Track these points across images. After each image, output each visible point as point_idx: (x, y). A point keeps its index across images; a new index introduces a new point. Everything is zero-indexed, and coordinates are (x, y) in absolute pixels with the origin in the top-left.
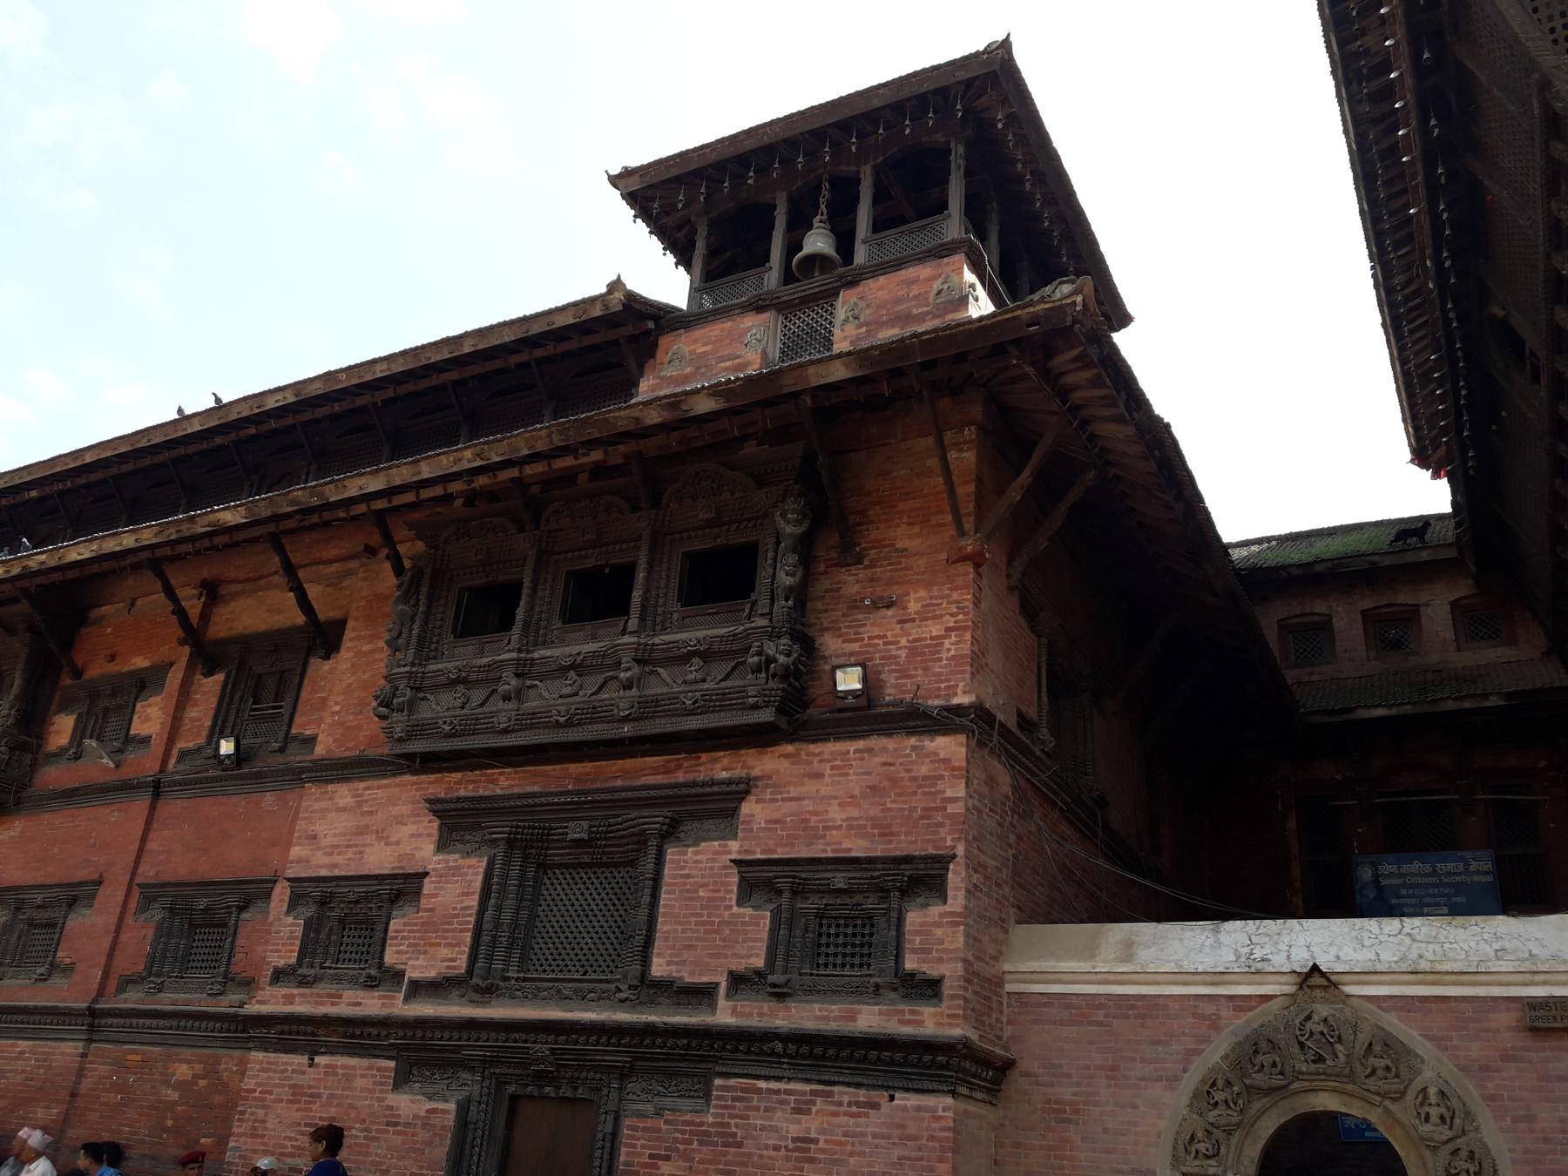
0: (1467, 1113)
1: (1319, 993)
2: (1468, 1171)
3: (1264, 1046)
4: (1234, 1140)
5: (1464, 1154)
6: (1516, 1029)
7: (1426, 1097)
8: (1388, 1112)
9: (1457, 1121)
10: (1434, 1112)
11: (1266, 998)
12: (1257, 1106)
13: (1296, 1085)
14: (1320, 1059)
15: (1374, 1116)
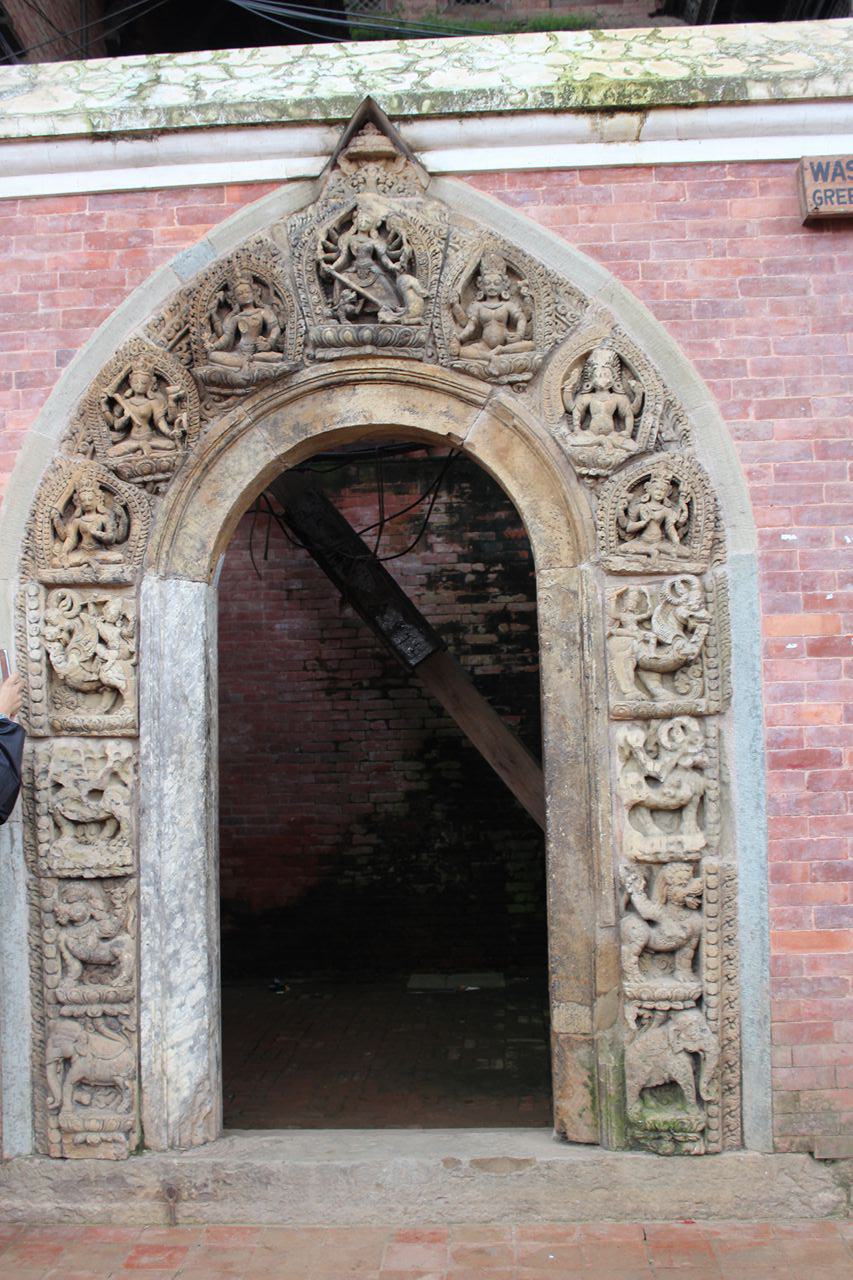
0: (669, 405)
1: (372, 171)
2: (663, 524)
3: (244, 289)
4: (163, 503)
5: (658, 488)
6: (779, 228)
7: (584, 377)
8: (502, 415)
9: (648, 420)
10: (602, 405)
11: (254, 188)
12: (217, 425)
13: (310, 373)
14: (365, 311)
15: (475, 433)
